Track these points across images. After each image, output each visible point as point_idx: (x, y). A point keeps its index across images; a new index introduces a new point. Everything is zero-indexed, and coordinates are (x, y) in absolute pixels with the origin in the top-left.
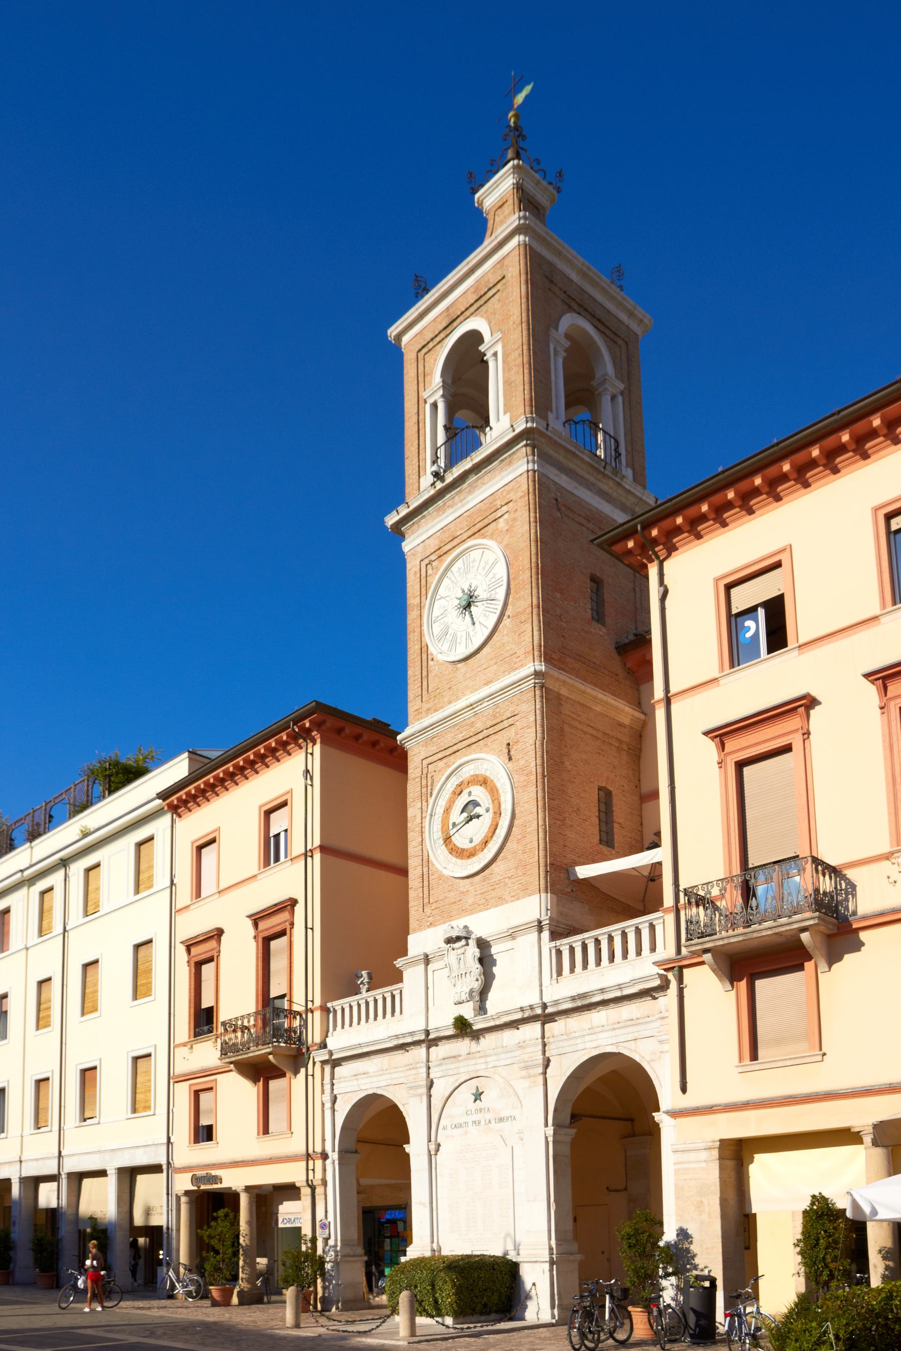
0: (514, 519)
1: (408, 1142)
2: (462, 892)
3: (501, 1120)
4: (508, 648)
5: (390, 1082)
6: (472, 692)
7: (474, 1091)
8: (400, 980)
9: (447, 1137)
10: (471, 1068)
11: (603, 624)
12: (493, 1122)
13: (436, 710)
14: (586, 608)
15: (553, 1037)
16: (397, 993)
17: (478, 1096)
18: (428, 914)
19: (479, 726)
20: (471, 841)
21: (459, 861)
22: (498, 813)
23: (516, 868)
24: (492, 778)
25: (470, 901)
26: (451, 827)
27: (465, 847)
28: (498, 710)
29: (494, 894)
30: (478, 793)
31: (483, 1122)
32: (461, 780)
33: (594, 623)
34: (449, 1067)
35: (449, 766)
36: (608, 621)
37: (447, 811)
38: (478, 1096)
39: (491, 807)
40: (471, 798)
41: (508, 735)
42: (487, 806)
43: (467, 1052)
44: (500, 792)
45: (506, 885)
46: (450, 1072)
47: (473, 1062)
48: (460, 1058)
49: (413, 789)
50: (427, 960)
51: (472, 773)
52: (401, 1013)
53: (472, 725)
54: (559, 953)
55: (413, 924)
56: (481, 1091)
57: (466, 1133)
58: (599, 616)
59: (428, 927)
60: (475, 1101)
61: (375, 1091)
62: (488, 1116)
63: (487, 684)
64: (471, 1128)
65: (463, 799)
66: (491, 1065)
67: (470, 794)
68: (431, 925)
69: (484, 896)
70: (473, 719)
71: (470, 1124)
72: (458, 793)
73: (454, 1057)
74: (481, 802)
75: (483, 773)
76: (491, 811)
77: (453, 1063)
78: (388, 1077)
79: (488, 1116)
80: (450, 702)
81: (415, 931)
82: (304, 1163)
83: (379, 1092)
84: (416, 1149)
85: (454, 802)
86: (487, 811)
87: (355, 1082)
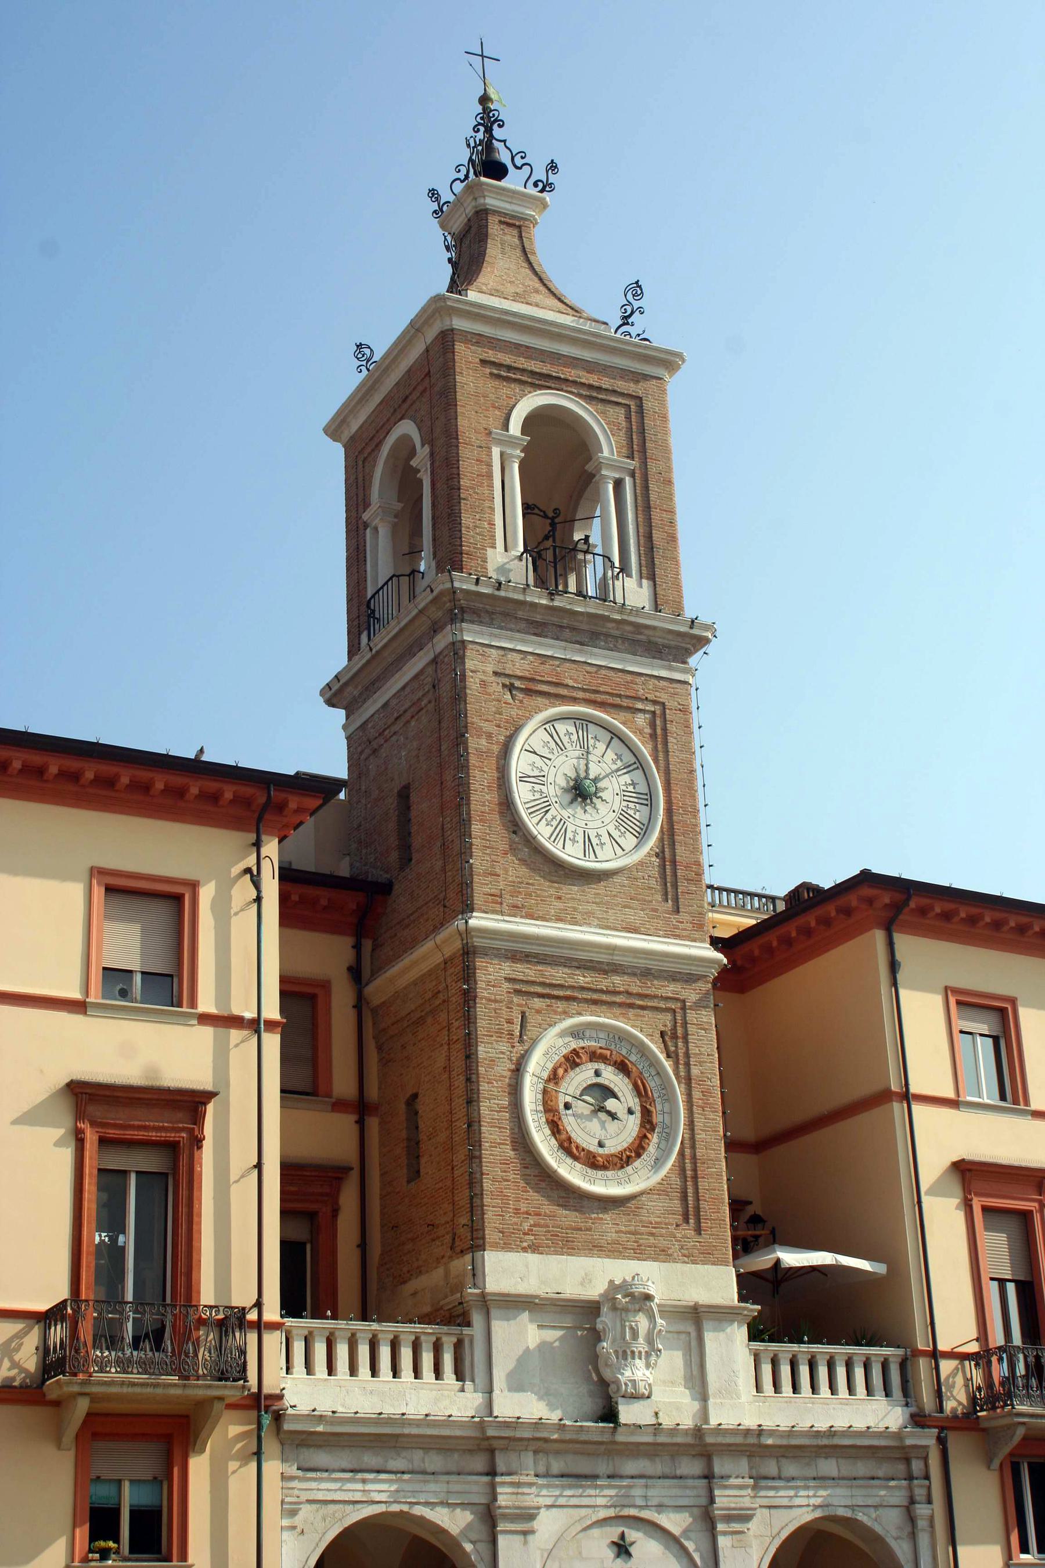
18: (526, 1226)
26: (561, 1106)
29: (652, 1240)
30: (610, 1076)
39: (637, 1109)
40: (599, 1080)
42: (631, 1104)
55: (491, 1235)
59: (524, 1250)
66: (655, 1502)
67: (597, 1073)
72: (572, 1061)
74: (620, 1094)
80: (559, 919)
81: (496, 1246)
87: (359, 1486)
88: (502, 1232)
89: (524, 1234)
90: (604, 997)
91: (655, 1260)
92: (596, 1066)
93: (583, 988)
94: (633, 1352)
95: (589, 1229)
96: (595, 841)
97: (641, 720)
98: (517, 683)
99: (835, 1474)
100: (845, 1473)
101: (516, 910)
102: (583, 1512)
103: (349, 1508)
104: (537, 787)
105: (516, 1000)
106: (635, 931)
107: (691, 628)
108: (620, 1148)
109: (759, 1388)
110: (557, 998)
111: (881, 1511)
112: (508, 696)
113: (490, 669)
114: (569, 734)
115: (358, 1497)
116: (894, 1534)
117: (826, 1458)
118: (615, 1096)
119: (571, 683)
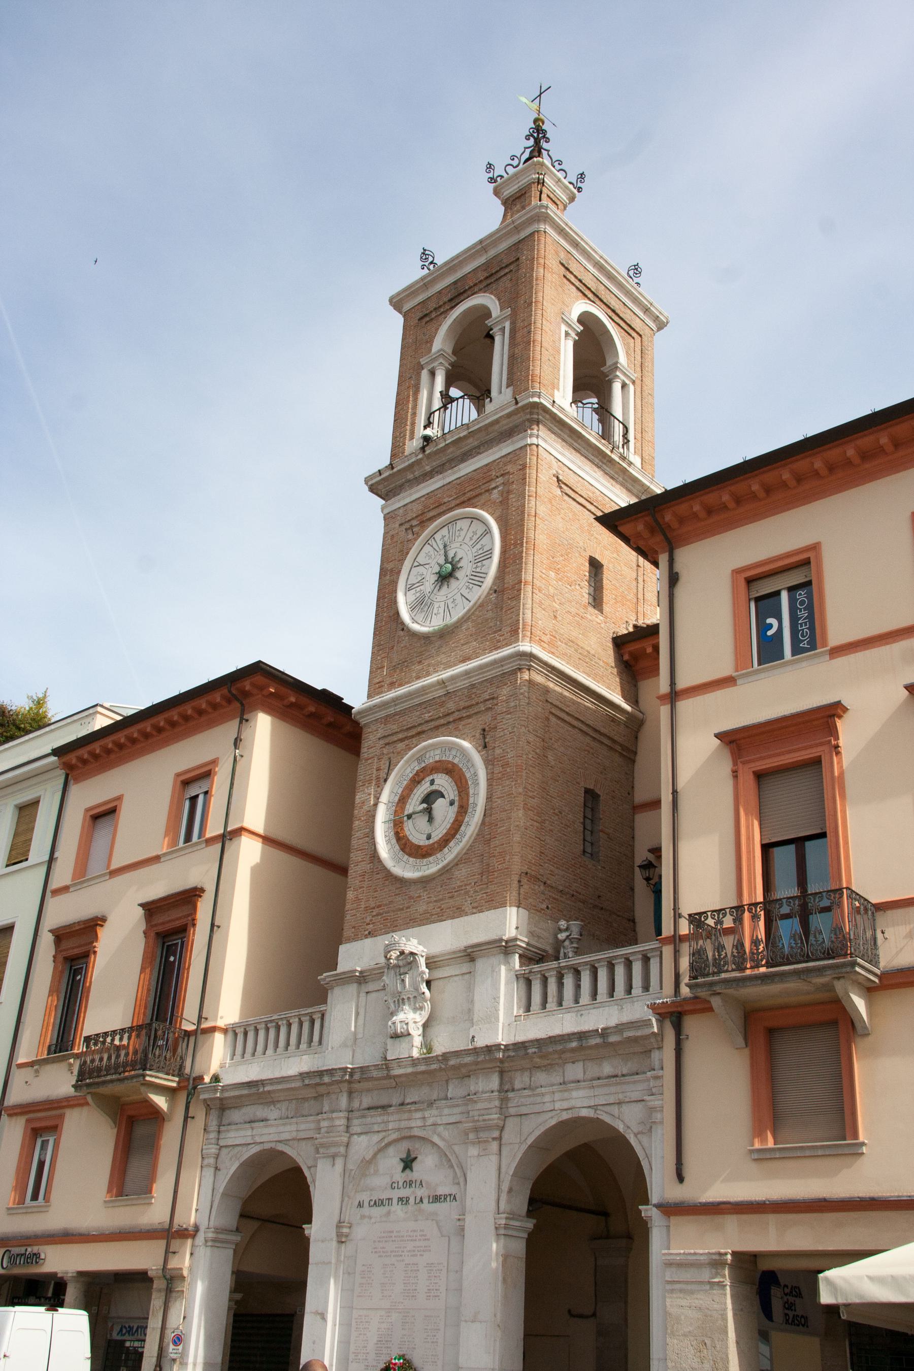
0: (509, 492)
1: (309, 1221)
2: (411, 898)
3: (437, 1199)
4: (491, 624)
5: (294, 1134)
6: (445, 669)
7: (404, 1156)
8: (324, 1001)
9: (363, 1217)
10: (404, 1124)
11: (601, 611)
12: (425, 1201)
13: (401, 685)
14: (583, 592)
15: (513, 1090)
16: (317, 1017)
17: (408, 1163)
19: (451, 706)
20: (429, 837)
21: (411, 859)
22: (463, 810)
23: (482, 874)
24: (461, 766)
25: (422, 907)
27: (421, 843)
28: (474, 690)
30: (443, 782)
31: (412, 1201)
32: (423, 765)
33: (591, 609)
34: (374, 1120)
35: (410, 749)
36: (606, 608)
37: (403, 800)
38: (408, 1163)
39: (457, 799)
40: (434, 787)
41: (487, 718)
42: (452, 797)
43: (400, 1101)
44: (470, 783)
45: (467, 893)
46: (376, 1128)
47: (406, 1116)
48: (391, 1110)
49: (364, 770)
50: (361, 979)
51: (437, 758)
52: (320, 1042)
53: (442, 704)
54: (529, 983)
55: (348, 932)
56: (413, 1156)
57: (389, 1213)
58: (597, 601)
59: (366, 937)
60: (404, 1169)
61: (273, 1145)
62: (420, 1192)
63: (464, 661)
64: (397, 1208)
65: (424, 788)
66: (430, 1121)
67: (432, 782)
68: (371, 934)
69: (439, 904)
70: (444, 699)
71: (395, 1201)
72: (416, 780)
73: (383, 1107)
75: (450, 759)
76: (456, 804)
77: (380, 1115)
78: (294, 1127)
79: (420, 1192)
80: (418, 678)
81: (349, 940)
82: (164, 1242)
83: (281, 1147)
84: (319, 1230)
85: (411, 790)
86: (452, 803)
87: (249, 1133)
88: (354, 927)
89: (368, 924)
90: (442, 721)
91: (453, 918)
92: (431, 778)
93: (427, 722)
94: (403, 999)
95: (408, 908)
96: (451, 606)
97: (495, 495)
98: (415, 523)
99: (580, 1076)
100: (589, 1075)
101: (392, 685)
102: (381, 1135)
103: (245, 1149)
104: (418, 589)
105: (385, 751)
106: (469, 659)
107: (517, 403)
108: (440, 836)
109: (528, 1009)
110: (412, 737)
111: (625, 1108)
112: (410, 536)
113: (397, 525)
114: (444, 537)
115: (249, 1140)
116: (636, 1131)
117: (573, 1063)
118: (443, 796)
119: (446, 500)
